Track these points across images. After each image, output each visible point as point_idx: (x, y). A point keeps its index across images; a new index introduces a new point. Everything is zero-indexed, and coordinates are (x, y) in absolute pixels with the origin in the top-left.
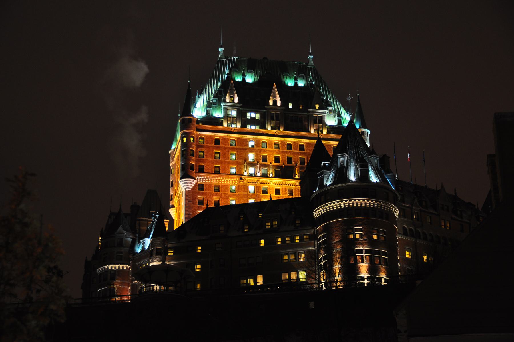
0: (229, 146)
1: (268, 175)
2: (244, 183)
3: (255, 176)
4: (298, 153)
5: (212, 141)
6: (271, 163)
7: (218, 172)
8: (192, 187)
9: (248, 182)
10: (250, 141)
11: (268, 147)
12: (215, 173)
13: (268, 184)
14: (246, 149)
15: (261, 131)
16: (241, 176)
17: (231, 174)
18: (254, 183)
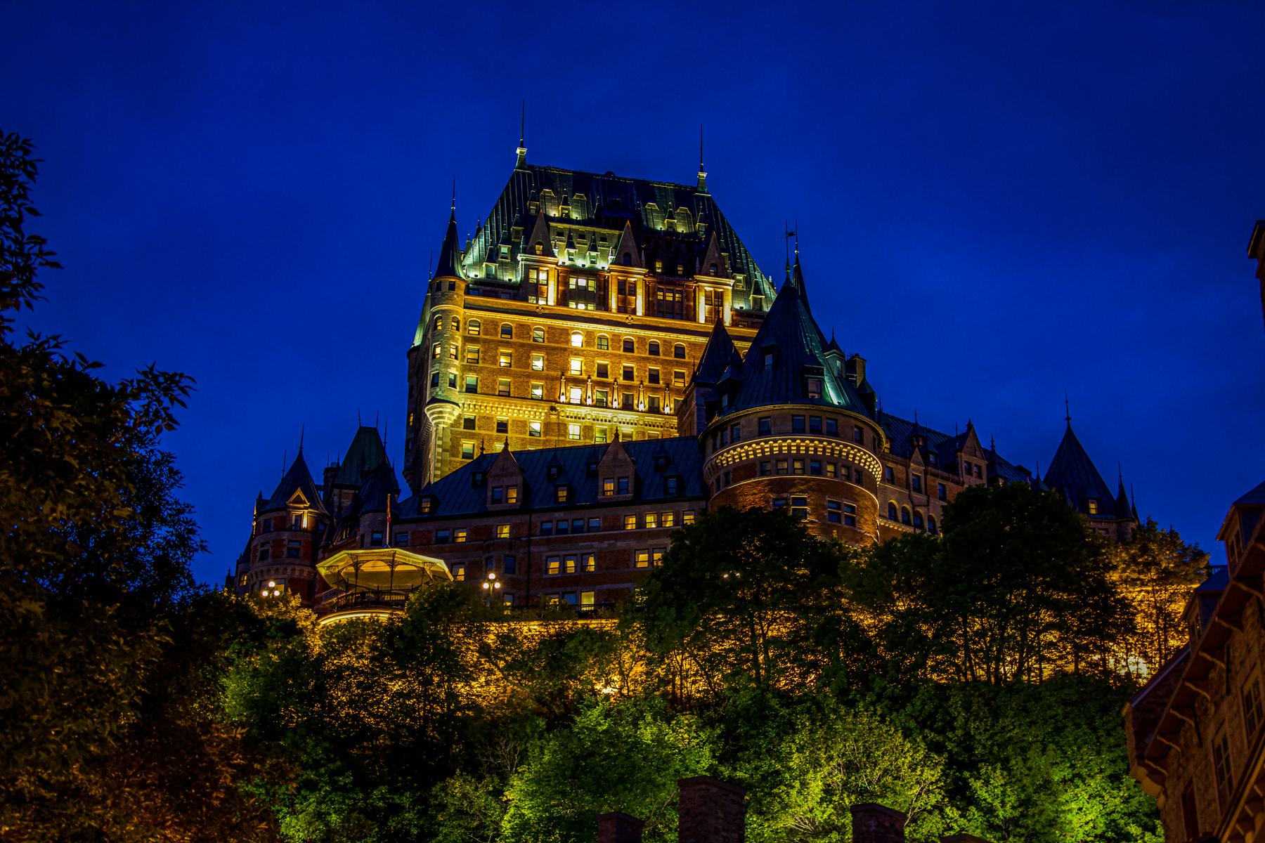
0: (531, 342)
1: (610, 404)
2: (558, 418)
3: (582, 404)
4: (671, 362)
5: (495, 329)
6: (615, 381)
7: (507, 394)
8: (450, 422)
9: (567, 417)
10: (574, 333)
11: (610, 348)
12: (499, 395)
13: (607, 423)
14: (565, 349)
15: (596, 315)
16: (553, 404)
17: (532, 399)
18: (579, 418)
